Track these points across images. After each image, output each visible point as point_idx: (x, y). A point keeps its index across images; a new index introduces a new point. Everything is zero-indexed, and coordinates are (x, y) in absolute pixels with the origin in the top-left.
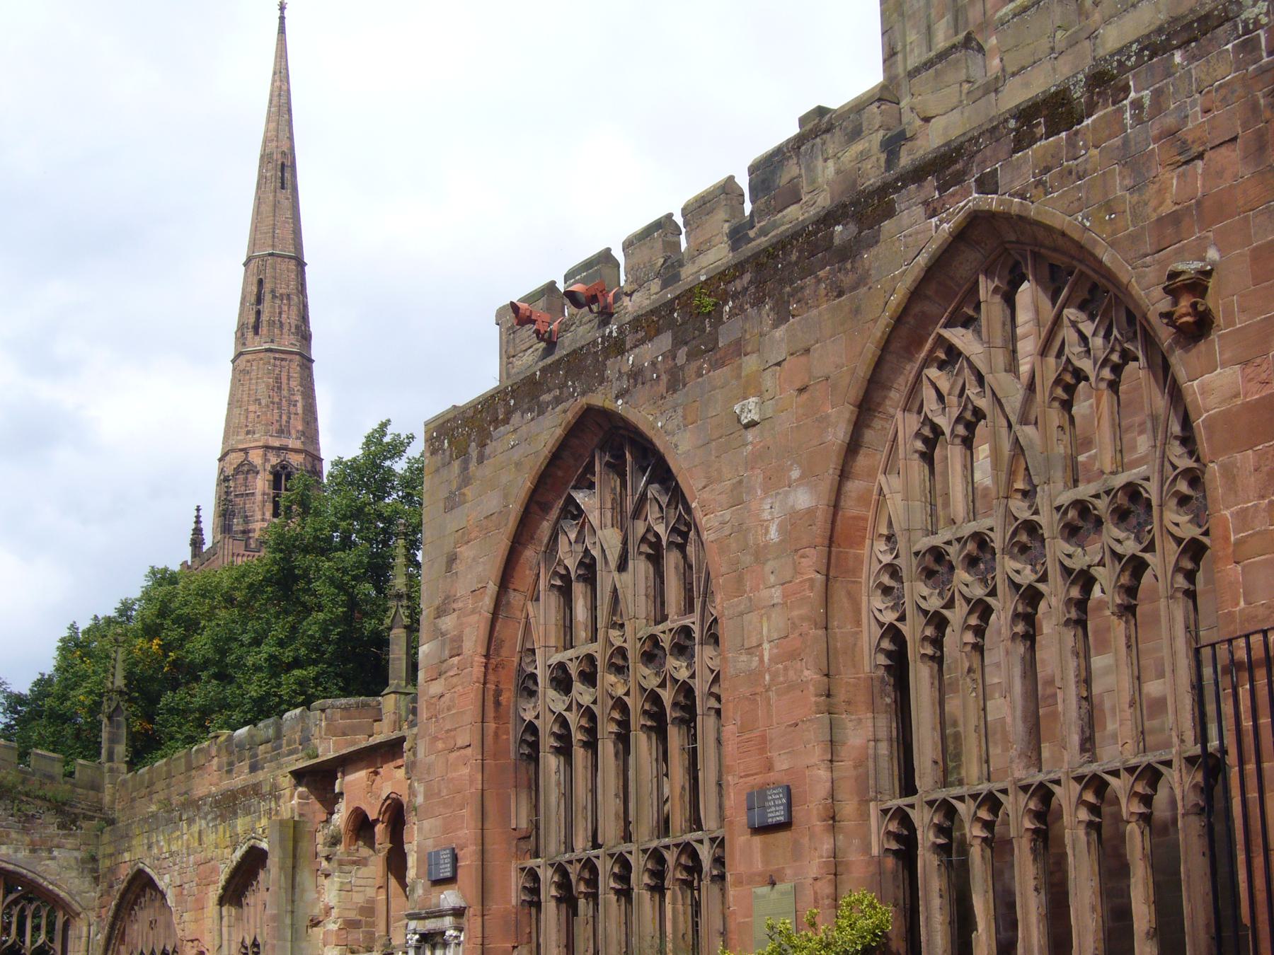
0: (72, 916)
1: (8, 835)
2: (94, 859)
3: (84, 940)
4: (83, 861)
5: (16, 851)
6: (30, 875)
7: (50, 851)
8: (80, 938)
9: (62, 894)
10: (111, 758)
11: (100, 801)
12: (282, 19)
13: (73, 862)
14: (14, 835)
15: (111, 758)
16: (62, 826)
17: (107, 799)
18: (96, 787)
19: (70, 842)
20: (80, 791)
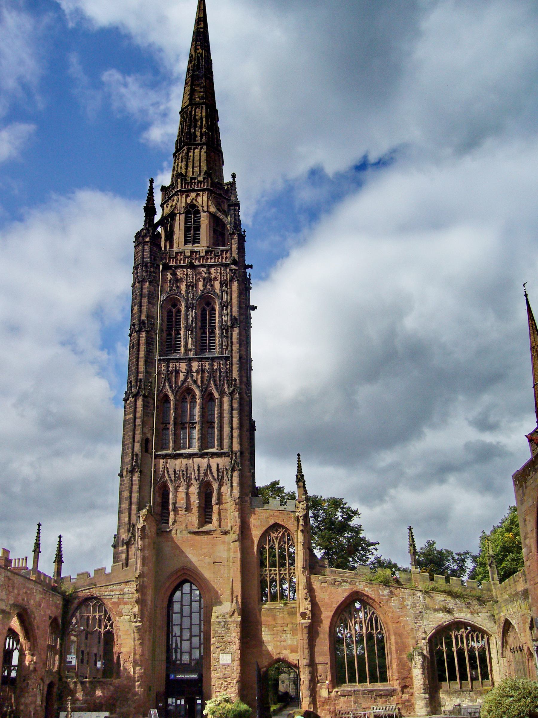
0: (489, 636)
1: (462, 610)
2: (494, 616)
3: (495, 644)
4: (490, 617)
5: (466, 615)
6: (472, 623)
7: (478, 614)
8: (493, 643)
9: (484, 629)
10: (493, 580)
11: (492, 595)
12: (527, 300)
13: (486, 617)
14: (464, 610)
15: (493, 580)
16: (480, 605)
17: (494, 594)
18: (490, 590)
19: (484, 610)
20: (484, 592)
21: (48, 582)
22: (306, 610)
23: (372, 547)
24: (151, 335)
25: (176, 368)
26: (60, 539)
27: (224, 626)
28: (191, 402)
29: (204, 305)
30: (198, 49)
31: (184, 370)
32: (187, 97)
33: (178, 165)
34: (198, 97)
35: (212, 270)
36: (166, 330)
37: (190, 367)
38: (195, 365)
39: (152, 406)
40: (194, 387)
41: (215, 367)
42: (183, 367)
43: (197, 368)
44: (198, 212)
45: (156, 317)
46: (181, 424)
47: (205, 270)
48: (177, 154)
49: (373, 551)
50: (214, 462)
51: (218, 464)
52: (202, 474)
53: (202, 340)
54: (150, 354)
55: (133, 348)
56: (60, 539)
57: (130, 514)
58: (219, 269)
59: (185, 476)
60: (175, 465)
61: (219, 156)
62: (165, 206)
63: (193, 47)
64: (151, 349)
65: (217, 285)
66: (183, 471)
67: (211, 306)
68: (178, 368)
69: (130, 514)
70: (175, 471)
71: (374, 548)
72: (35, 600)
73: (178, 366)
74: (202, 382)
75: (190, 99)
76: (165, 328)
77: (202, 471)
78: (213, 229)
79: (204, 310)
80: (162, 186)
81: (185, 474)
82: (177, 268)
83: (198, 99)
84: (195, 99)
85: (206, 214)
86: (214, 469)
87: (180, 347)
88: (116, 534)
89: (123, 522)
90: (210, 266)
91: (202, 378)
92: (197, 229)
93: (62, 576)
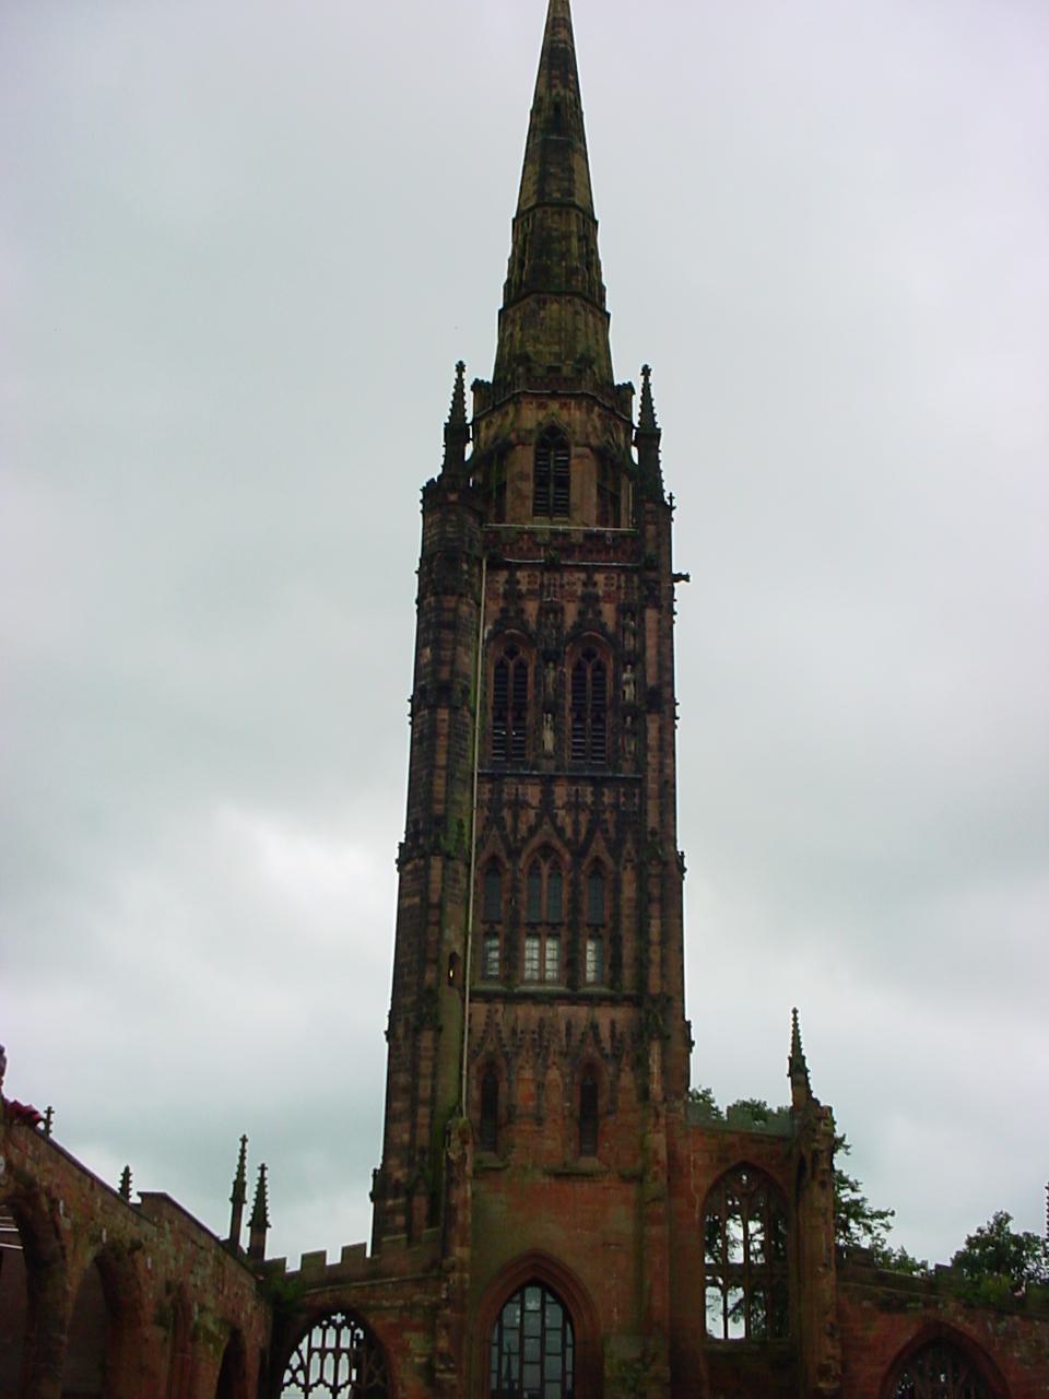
21: (908, 1305)
22: (831, 1361)
23: (878, 1221)
24: (463, 716)
25: (517, 795)
26: (262, 1173)
27: (633, 1389)
28: (550, 876)
29: (580, 656)
30: (555, 86)
31: (535, 802)
32: (531, 188)
33: (511, 335)
34: (558, 190)
35: (600, 578)
36: (493, 709)
37: (547, 795)
38: (561, 793)
39: (465, 880)
40: (557, 844)
41: (606, 800)
42: (533, 794)
43: (565, 799)
44: (564, 446)
45: (473, 677)
46: (528, 924)
47: (583, 576)
48: (510, 312)
49: (882, 1230)
50: (605, 1017)
51: (613, 1023)
52: (575, 1042)
53: (575, 737)
54: (461, 760)
55: (421, 744)
56: (262, 1173)
57: (414, 1126)
58: (615, 576)
59: (537, 1043)
60: (516, 1018)
61: (603, 323)
62: (483, 424)
63: (543, 80)
64: (461, 749)
65: (608, 611)
66: (534, 1032)
67: (594, 661)
68: (521, 797)
69: (414, 1126)
70: (514, 1031)
71: (882, 1225)
72: (246, 1312)
73: (520, 791)
74: (576, 832)
75: (541, 193)
76: (490, 701)
77: (577, 1033)
78: (598, 484)
79: (578, 668)
80: (477, 380)
81: (539, 1041)
82: (519, 566)
83: (557, 195)
84: (551, 195)
85: (580, 450)
86: (605, 1032)
87: (523, 749)
88: (379, 1167)
89: (398, 1141)
90: (597, 569)
91: (576, 823)
92: (563, 483)
93: (267, 1257)
